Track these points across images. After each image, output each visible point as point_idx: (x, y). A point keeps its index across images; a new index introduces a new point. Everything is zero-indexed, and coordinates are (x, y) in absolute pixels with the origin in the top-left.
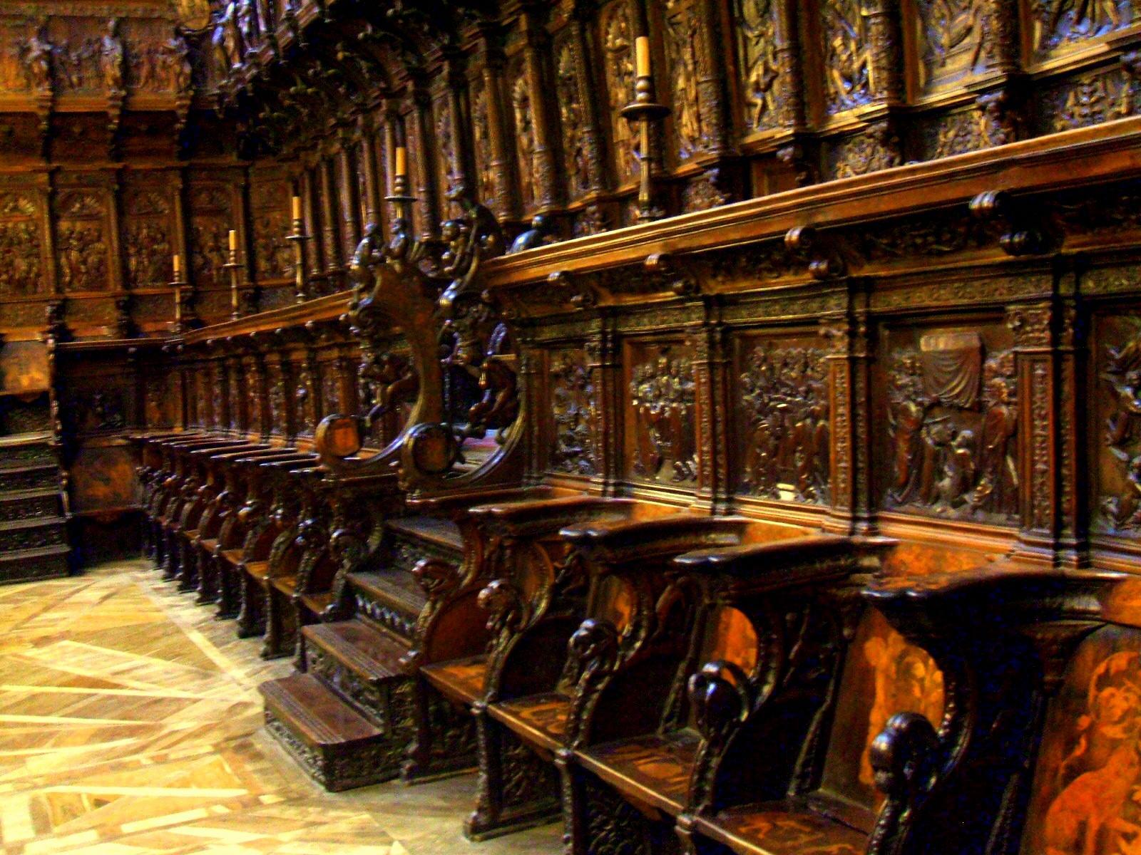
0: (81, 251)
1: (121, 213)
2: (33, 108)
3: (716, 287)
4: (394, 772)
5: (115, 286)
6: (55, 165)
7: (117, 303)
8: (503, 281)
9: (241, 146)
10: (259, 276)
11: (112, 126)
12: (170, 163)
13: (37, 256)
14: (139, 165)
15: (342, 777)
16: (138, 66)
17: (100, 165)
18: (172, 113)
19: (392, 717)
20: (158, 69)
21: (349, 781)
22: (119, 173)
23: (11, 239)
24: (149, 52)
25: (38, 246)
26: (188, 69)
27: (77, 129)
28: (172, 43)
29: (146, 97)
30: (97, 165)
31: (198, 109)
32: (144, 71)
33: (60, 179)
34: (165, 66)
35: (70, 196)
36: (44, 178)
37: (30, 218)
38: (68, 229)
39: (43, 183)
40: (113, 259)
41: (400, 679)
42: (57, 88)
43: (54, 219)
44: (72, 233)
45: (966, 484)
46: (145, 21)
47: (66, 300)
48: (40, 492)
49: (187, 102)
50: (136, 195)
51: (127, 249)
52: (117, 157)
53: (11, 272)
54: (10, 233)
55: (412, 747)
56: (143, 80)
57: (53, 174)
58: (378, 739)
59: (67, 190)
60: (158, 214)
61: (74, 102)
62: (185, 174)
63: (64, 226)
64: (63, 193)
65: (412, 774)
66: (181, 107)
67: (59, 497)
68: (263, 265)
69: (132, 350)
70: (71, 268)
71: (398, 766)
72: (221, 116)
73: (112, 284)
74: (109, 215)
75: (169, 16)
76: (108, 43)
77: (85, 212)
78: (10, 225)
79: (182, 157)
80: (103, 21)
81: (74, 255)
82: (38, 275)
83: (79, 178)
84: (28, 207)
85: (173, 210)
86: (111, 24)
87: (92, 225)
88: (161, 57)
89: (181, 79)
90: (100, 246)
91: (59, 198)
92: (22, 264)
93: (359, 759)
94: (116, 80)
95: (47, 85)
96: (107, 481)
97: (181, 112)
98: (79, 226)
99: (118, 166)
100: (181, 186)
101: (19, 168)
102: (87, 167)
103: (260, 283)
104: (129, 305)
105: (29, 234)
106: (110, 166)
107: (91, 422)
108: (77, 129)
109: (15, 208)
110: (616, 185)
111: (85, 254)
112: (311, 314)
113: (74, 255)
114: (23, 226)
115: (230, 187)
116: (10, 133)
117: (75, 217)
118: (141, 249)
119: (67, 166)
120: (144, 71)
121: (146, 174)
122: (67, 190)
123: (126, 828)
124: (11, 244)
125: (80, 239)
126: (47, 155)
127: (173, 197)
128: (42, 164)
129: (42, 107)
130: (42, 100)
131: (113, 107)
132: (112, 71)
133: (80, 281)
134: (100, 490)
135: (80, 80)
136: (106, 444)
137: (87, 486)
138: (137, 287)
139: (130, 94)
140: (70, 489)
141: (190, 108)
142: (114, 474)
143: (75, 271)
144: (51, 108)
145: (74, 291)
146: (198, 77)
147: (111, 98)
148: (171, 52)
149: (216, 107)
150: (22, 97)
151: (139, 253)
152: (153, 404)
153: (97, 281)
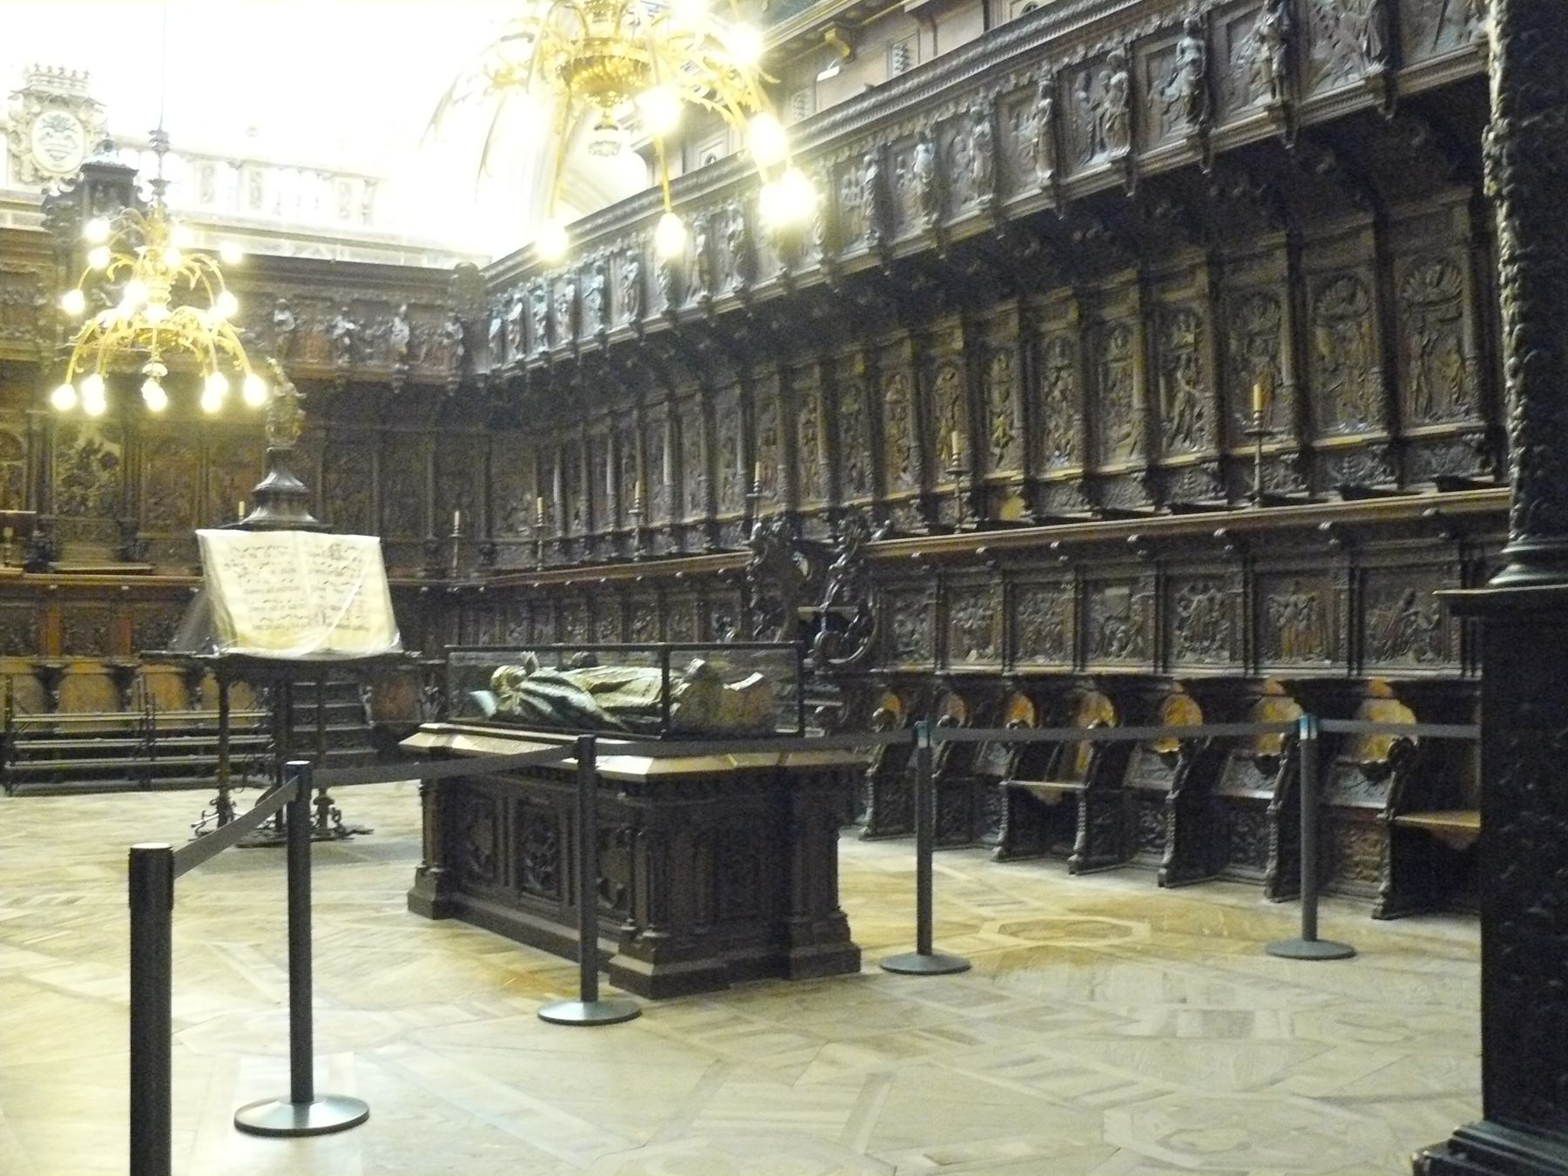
3: (1009, 565)
8: (871, 556)
10: (494, 533)
18: (441, 389)
26: (461, 351)
28: (450, 327)
43: (326, 470)
45: (1122, 648)
46: (427, 308)
49: (458, 379)
56: (422, 356)
69: (424, 589)
80: (398, 306)
81: (339, 502)
86: (404, 308)
96: (393, 699)
97: (451, 387)
110: (884, 493)
128: (322, 423)
148: (449, 335)
152: (432, 637)
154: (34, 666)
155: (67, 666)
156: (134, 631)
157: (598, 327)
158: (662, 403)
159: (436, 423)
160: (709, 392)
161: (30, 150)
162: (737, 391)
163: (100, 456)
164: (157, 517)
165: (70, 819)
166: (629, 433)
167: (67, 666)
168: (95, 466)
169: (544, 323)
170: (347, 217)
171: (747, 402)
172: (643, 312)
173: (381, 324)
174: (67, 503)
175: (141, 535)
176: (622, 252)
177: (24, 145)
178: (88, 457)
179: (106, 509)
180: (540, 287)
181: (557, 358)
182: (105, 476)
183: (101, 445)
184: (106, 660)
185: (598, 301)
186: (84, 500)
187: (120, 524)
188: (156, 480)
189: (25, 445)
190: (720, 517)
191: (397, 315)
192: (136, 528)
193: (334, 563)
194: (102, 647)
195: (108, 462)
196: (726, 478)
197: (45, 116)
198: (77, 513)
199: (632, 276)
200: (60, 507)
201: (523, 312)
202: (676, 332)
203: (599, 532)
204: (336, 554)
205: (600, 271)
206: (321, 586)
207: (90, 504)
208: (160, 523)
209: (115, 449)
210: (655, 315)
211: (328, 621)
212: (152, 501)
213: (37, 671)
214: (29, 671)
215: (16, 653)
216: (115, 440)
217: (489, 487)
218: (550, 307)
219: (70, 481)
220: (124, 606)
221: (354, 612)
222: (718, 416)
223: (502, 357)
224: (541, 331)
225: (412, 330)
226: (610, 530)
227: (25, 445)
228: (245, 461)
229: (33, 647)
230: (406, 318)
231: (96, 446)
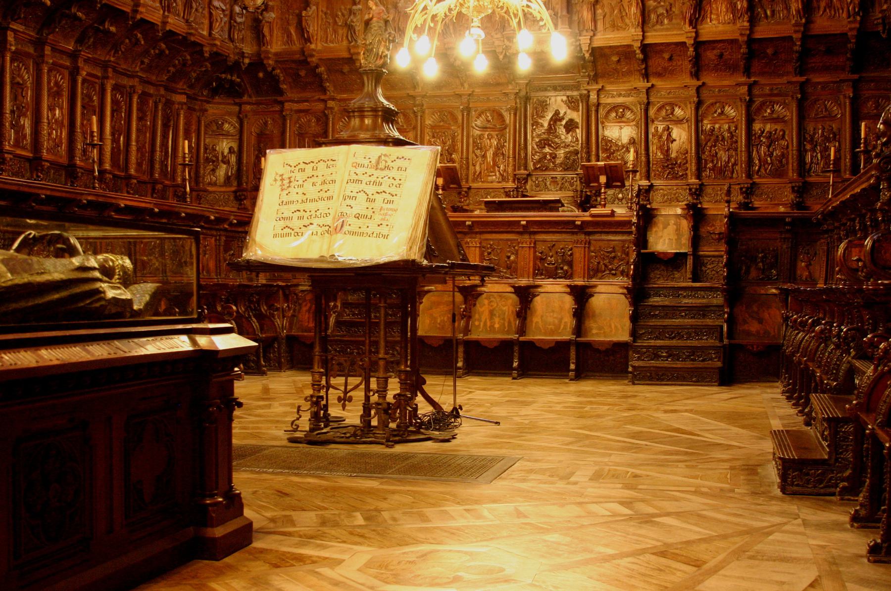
0: (769, 147)
1: (802, 117)
2: (736, 36)
4: (832, 490)
5: (792, 174)
6: (753, 79)
7: (793, 188)
11: (796, 48)
12: (843, 76)
13: (736, 150)
14: (817, 79)
15: (792, 485)
17: (787, 80)
18: (844, 35)
19: (835, 446)
21: (795, 488)
22: (803, 85)
23: (717, 137)
25: (736, 142)
27: (770, 51)
29: (822, 24)
30: (784, 80)
31: (865, 34)
33: (756, 91)
35: (763, 104)
36: (744, 89)
37: (732, 121)
38: (760, 129)
39: (744, 94)
40: (793, 153)
41: (845, 421)
42: (753, 21)
43: (750, 122)
44: (763, 132)
47: (754, 184)
48: (709, 322)
50: (815, 102)
51: (804, 145)
52: (801, 72)
53: (715, 162)
54: (716, 132)
55: (847, 473)
57: (751, 87)
58: (823, 462)
59: (761, 99)
60: (832, 118)
61: (763, 31)
62: (856, 85)
63: (757, 126)
64: (758, 101)
65: (844, 491)
66: (851, 29)
67: (722, 327)
70: (760, 160)
71: (836, 486)
72: (884, 36)
73: (790, 174)
74: (792, 119)
77: (775, 116)
78: (717, 126)
79: (853, 71)
81: (763, 149)
82: (735, 164)
83: (771, 90)
84: (730, 111)
85: (843, 115)
87: (778, 127)
90: (784, 143)
91: (755, 106)
92: (723, 156)
93: (808, 474)
94: (798, 11)
95: (746, 18)
96: (760, 321)
98: (768, 127)
99: (803, 79)
100: (851, 95)
101: (726, 83)
102: (778, 81)
104: (803, 189)
105: (731, 133)
106: (794, 79)
107: (753, 274)
108: (770, 51)
109: (722, 113)
111: (771, 149)
113: (763, 149)
114: (726, 127)
116: (721, 56)
117: (766, 120)
118: (816, 146)
119: (762, 80)
121: (825, 85)
122: (761, 99)
123: (640, 487)
124: (716, 141)
125: (768, 138)
126: (747, 72)
127: (845, 103)
128: (743, 79)
129: (741, 35)
130: (743, 29)
131: (796, 32)
133: (766, 170)
134: (754, 327)
136: (763, 292)
137: (745, 322)
138: (811, 176)
139: (809, 22)
140: (731, 321)
141: (859, 30)
142: (766, 316)
143: (763, 162)
144: (749, 36)
145: (760, 177)
147: (795, 25)
149: (880, 28)
150: (728, 28)
151: (813, 150)
153: (779, 172)
163: (564, 122)
174: (539, 161)
186: (554, 157)
193: (377, 173)
198: (547, 169)
200: (534, 164)
204: (382, 165)
206: (354, 194)
207: (558, 161)
211: (346, 228)
219: (543, 144)
221: (377, 218)
228: (681, 118)
231: (561, 115)
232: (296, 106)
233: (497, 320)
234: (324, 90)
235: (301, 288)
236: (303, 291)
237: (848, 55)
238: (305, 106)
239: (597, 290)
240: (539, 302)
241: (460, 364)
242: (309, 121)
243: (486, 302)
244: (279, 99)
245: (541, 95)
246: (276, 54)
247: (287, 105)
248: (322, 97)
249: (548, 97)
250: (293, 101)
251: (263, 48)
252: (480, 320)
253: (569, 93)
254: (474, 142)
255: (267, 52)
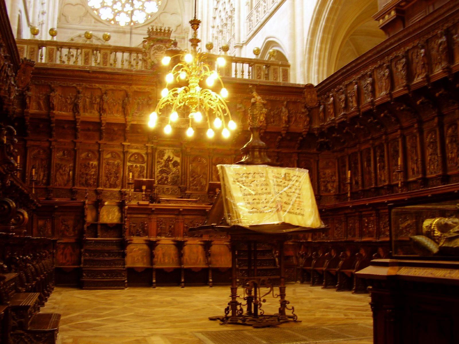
9: (318, 146)
16: (292, 117)
18: (300, 134)
20: (298, 118)
24: (295, 113)
26: (308, 119)
28: (303, 110)
31: (310, 134)
32: (293, 119)
34: (300, 118)
49: (307, 130)
66: (304, 131)
68: (322, 188)
75: (303, 101)
76: (284, 109)
80: (283, 102)
86: (285, 103)
88: (298, 115)
89: (306, 123)
94: (286, 121)
97: (304, 133)
103: (322, 194)
112: (431, 192)
115: (312, 160)
120: (293, 119)
131: (284, 130)
132: (284, 118)
135: (274, 122)
146: (310, 122)
147: (283, 127)
148: (303, 113)
149: (316, 132)
154: (146, 241)
155: (159, 240)
156: (184, 227)
157: (369, 100)
158: (397, 131)
159: (298, 149)
160: (421, 123)
161: (150, 58)
162: (436, 120)
163: (172, 162)
164: (193, 186)
165: (156, 306)
166: (381, 146)
167: (159, 240)
168: (171, 166)
169: (344, 102)
170: (260, 78)
171: (441, 125)
172: (392, 88)
173: (277, 109)
175: (187, 192)
176: (381, 66)
177: (148, 57)
178: (168, 163)
179: (174, 183)
180: (341, 89)
181: (349, 116)
182: (174, 170)
183: (173, 158)
184: (173, 238)
185: (370, 88)
186: (167, 178)
187: (179, 187)
188: (193, 171)
189: (146, 158)
190: (429, 176)
191: (283, 105)
192: (186, 189)
194: (172, 233)
195: (175, 164)
196: (430, 160)
197: (155, 46)
198: (164, 184)
199: (387, 74)
200: (158, 181)
201: (334, 100)
202: (410, 95)
203: (367, 188)
205: (370, 76)
207: (169, 181)
208: (194, 187)
209: (178, 160)
210: (397, 89)
212: (191, 179)
213: (147, 242)
214: (144, 242)
215: (139, 235)
216: (178, 156)
217: (318, 173)
218: (346, 96)
219: (162, 172)
220: (181, 217)
222: (425, 134)
223: (324, 120)
224: (343, 106)
225: (289, 111)
226: (373, 186)
227: (146, 158)
229: (146, 233)
230: (286, 107)
231: (171, 159)
232: (32, 143)
233: (166, 258)
234: (51, 136)
235: (59, 241)
236: (59, 243)
237: (298, 142)
238: (38, 143)
239: (188, 243)
240: (186, 249)
241: (154, 281)
242: (39, 151)
243: (160, 249)
244: (25, 138)
245: (162, 148)
246: (32, 114)
247: (29, 143)
248: (50, 139)
249: (165, 149)
250: (32, 140)
251: (25, 110)
252: (157, 258)
253: (175, 148)
254: (129, 169)
255: (28, 112)
